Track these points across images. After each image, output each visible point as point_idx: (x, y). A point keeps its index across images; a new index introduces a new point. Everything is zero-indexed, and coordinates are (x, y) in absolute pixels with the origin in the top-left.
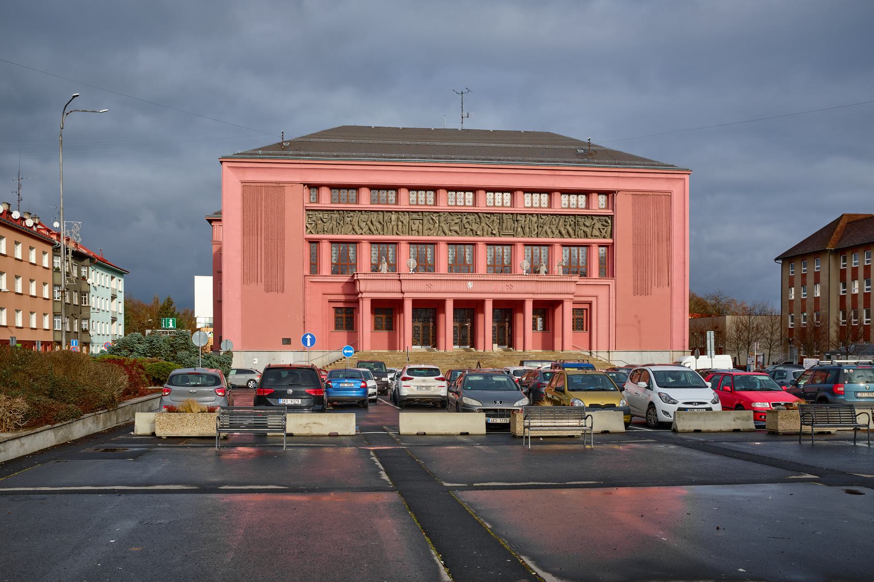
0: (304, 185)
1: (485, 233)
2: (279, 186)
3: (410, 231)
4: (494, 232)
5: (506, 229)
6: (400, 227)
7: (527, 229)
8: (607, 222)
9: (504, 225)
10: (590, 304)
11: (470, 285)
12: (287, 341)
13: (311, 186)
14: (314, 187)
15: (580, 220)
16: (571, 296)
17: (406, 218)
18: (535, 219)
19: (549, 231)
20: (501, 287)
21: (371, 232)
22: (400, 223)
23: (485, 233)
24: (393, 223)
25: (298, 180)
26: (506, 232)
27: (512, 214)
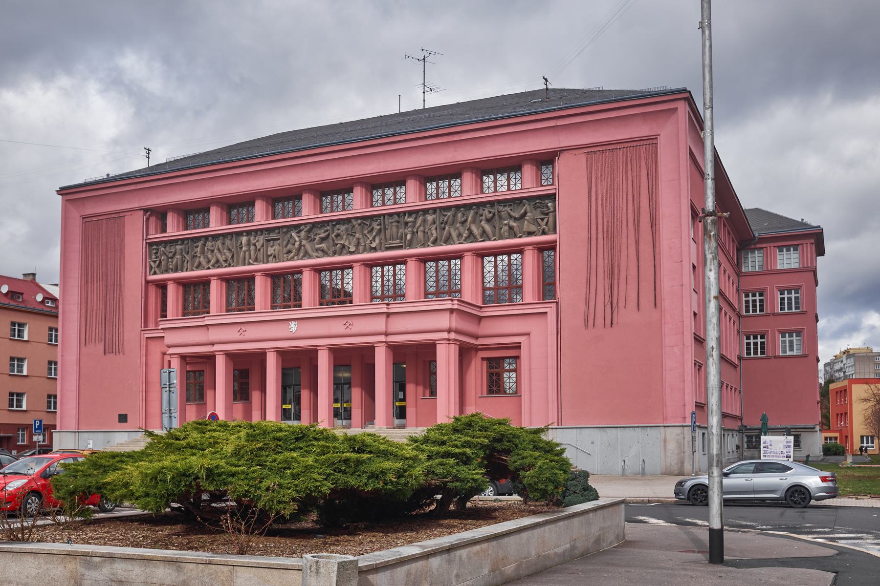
0: (146, 210)
1: (361, 248)
2: (119, 216)
3: (267, 259)
4: (373, 245)
5: (392, 238)
6: (252, 252)
7: (420, 234)
8: (547, 207)
9: (388, 232)
10: (518, 346)
11: (293, 326)
12: (123, 418)
13: (150, 212)
14: (159, 214)
15: (501, 208)
16: (445, 335)
17: (261, 239)
18: (430, 218)
19: (454, 235)
20: (338, 327)
21: (217, 265)
22: (252, 248)
23: (361, 248)
24: (244, 248)
25: (136, 205)
26: (392, 243)
27: (398, 214)
